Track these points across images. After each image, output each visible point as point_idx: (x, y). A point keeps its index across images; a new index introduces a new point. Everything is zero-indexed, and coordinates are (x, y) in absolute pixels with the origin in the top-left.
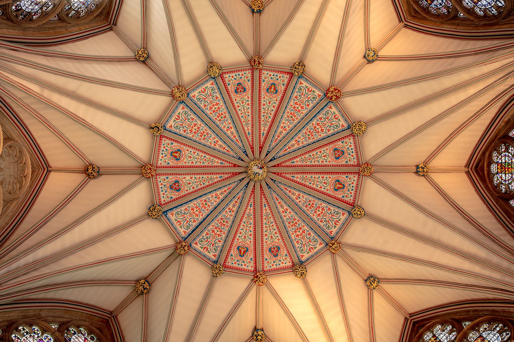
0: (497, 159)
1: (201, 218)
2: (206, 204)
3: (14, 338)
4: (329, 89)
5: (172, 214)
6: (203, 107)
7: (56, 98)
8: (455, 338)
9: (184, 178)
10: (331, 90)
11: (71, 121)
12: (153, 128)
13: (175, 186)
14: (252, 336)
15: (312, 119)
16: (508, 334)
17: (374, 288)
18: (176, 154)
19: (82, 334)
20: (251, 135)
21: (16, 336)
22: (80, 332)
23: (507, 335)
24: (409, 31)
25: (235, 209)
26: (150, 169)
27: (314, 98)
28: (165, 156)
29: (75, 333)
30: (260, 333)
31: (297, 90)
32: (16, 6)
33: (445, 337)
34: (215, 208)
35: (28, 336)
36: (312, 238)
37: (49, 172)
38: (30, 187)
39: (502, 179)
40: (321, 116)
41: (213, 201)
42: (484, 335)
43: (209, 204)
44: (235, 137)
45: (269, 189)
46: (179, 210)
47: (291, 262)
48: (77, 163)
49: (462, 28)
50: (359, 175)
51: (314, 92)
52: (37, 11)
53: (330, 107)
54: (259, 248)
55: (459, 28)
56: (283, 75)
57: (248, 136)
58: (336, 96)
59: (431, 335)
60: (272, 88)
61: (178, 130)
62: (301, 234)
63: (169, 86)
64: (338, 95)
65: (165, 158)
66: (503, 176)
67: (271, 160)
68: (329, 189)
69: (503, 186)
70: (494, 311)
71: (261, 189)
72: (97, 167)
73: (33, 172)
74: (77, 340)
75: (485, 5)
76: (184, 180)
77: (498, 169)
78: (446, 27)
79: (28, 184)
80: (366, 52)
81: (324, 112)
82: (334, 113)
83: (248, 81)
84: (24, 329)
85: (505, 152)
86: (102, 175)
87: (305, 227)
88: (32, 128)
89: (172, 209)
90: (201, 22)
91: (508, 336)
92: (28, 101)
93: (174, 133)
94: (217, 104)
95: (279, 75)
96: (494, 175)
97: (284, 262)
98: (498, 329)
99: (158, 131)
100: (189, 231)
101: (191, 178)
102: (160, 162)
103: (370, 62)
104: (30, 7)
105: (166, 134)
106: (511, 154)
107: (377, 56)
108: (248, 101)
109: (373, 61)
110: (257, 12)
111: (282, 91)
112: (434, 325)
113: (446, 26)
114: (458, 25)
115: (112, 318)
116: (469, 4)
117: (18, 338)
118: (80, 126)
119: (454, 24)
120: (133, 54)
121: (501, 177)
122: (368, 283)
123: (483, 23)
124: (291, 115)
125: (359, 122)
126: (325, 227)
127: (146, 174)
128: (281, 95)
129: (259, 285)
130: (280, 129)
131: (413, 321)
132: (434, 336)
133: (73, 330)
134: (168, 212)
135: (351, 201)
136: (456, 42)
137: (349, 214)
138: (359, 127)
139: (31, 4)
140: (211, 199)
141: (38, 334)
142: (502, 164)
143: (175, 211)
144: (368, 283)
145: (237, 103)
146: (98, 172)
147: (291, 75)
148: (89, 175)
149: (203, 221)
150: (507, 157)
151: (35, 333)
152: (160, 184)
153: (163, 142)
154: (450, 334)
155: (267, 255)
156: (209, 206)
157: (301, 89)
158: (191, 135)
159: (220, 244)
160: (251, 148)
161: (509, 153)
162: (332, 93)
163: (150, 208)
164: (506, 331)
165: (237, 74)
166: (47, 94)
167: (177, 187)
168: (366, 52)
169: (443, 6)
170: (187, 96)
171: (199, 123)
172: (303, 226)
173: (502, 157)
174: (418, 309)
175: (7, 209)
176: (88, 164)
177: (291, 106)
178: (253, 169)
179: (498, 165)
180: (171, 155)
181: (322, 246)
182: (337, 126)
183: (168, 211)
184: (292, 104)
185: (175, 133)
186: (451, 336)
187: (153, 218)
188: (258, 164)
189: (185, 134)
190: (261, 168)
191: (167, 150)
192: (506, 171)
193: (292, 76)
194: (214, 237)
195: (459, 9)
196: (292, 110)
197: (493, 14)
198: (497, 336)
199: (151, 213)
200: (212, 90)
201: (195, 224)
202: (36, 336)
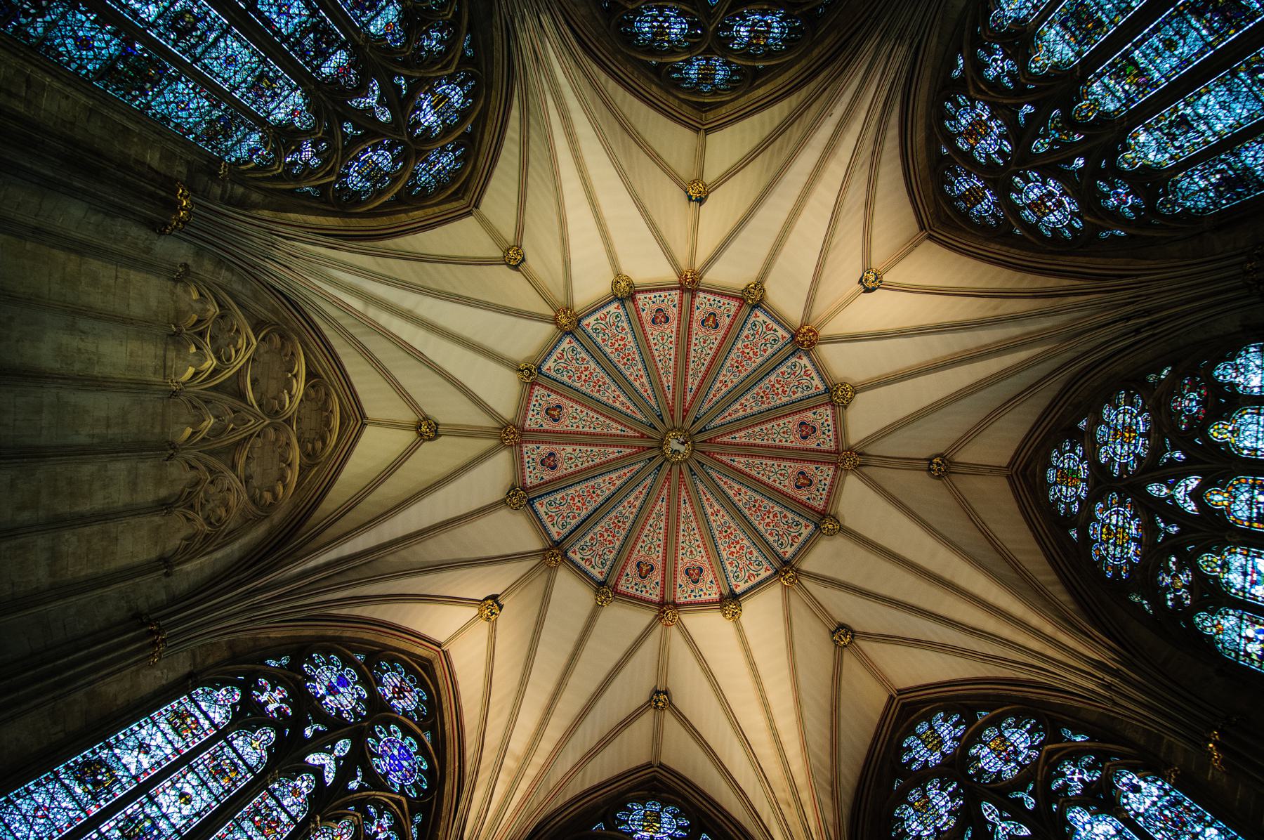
0: (1057, 461)
1: (584, 513)
2: (594, 492)
3: (306, 669)
4: (800, 329)
5: (542, 504)
6: (601, 341)
7: (384, 319)
8: (962, 735)
9: (564, 449)
10: (803, 330)
11: (402, 354)
12: (523, 371)
13: (549, 462)
14: (650, 701)
15: (769, 372)
16: (1042, 735)
17: (845, 646)
18: (554, 413)
19: (397, 672)
20: (671, 390)
21: (308, 667)
22: (394, 669)
23: (1040, 736)
24: (935, 246)
25: (638, 504)
26: (514, 433)
27: (775, 340)
28: (538, 414)
29: (388, 670)
30: (662, 697)
31: (750, 326)
32: (340, 184)
33: (947, 731)
34: (608, 500)
35: (324, 668)
36: (754, 559)
37: (364, 425)
38: (336, 446)
39: (1061, 494)
40: (784, 369)
42: (1007, 734)
43: (599, 492)
44: (646, 391)
46: (552, 499)
47: (718, 594)
48: (409, 416)
49: (1018, 251)
50: (836, 467)
51: (775, 330)
52: (368, 190)
53: (800, 358)
54: (670, 568)
55: (1012, 250)
56: (729, 301)
58: (810, 341)
59: (926, 726)
60: (711, 320)
62: (738, 552)
63: (552, 306)
64: (813, 339)
65: (536, 417)
66: (1064, 489)
67: (700, 432)
68: (787, 486)
69: (1063, 506)
70: (1026, 699)
72: (435, 423)
73: (342, 424)
74: (390, 680)
75: (1054, 223)
77: (1057, 477)
78: (994, 247)
79: (334, 442)
80: (863, 275)
81: (790, 364)
82: (805, 367)
83: (674, 306)
84: (319, 658)
85: (1069, 451)
86: (441, 435)
87: (745, 542)
88: (346, 362)
89: (543, 495)
90: (607, 212)
91: (1042, 738)
92: (345, 321)
93: (553, 379)
94: (623, 339)
95: (722, 301)
96: (1051, 485)
97: (708, 592)
98: (1028, 726)
99: (530, 375)
100: (565, 532)
101: (574, 450)
102: (528, 422)
103: (868, 290)
104: (360, 184)
105: (542, 380)
106: (1079, 457)
107: (880, 282)
108: (671, 337)
109: (873, 290)
110: (696, 200)
111: (726, 326)
112: (934, 712)
113: (992, 245)
114: (1012, 246)
115: (442, 653)
116: (1030, 217)
117: (312, 670)
118: (414, 362)
119: (1005, 244)
120: (501, 254)
121: (1060, 491)
122: (836, 638)
123: (1050, 248)
124: (736, 364)
125: (842, 385)
126: (776, 544)
128: (723, 331)
129: (666, 625)
130: (718, 385)
131: (901, 702)
132: (931, 727)
133: (385, 665)
135: (821, 508)
136: (1007, 273)
137: (816, 527)
138: (842, 392)
139: (361, 180)
140: (602, 485)
141: (338, 667)
142: (1063, 471)
143: (546, 500)
144: (836, 638)
145: (654, 339)
146: (436, 431)
147: (742, 302)
148: (421, 435)
149: (588, 518)
150: (1072, 461)
151: (334, 665)
152: (526, 456)
154: (955, 728)
155: (682, 579)
156: (598, 495)
157: (755, 325)
158: (579, 385)
159: (611, 556)
160: (670, 411)
161: (1076, 454)
162: (804, 336)
163: (509, 492)
164: (1039, 730)
165: (657, 294)
166: (372, 312)
167: (552, 463)
168: (863, 275)
169: (989, 215)
170: (578, 325)
171: (593, 366)
172: (742, 540)
173: (1064, 459)
174: (911, 684)
175: (304, 479)
176: (421, 418)
177: (738, 349)
178: (671, 445)
179: (1057, 471)
180: (547, 412)
181: (768, 573)
182: (808, 387)
183: (535, 498)
184: (739, 346)
185: (555, 380)
186: (957, 730)
187: (512, 508)
189: (569, 382)
190: (683, 444)
191: (540, 404)
192: (1068, 483)
193: (743, 305)
194: (602, 544)
195: (1013, 223)
196: (738, 356)
197: (1065, 237)
198: (1024, 736)
200: (617, 317)
201: (574, 522)
202: (335, 669)
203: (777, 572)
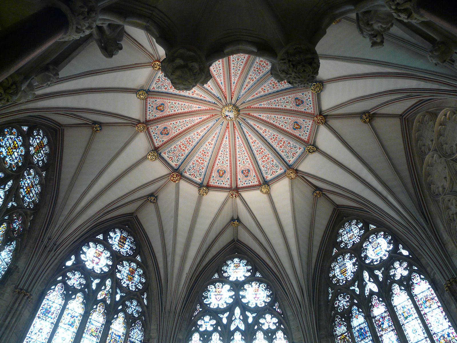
9: (291, 107)
12: (313, 151)
20: (237, 137)
41: (267, 87)
43: (270, 85)
57: (238, 136)
61: (295, 145)
71: (225, 96)
76: (292, 106)
101: (285, 106)
127: (322, 119)
140: (269, 88)
153: (307, 137)
156: (271, 84)
188: (230, 119)
190: (227, 116)
199: (320, 88)
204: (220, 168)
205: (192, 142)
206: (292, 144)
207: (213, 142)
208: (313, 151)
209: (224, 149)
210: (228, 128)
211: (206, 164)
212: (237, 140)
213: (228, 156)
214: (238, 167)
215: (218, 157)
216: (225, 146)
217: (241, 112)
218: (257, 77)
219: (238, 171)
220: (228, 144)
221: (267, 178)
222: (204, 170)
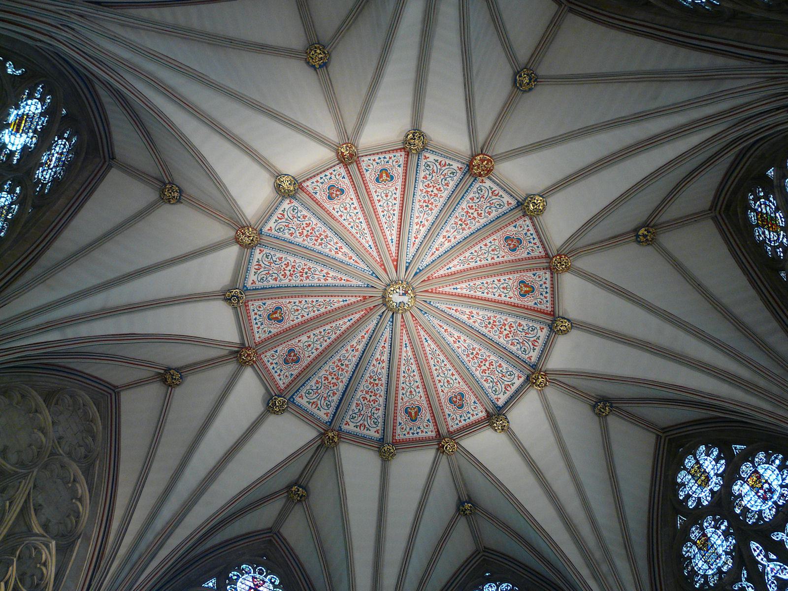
2: (342, 365)
5: (301, 397)
9: (299, 341)
20: (374, 249)
41: (350, 357)
43: (346, 362)
45: (425, 315)
76: (299, 344)
101: (309, 337)
134: (294, 397)
140: (347, 355)
156: (347, 366)
188: (398, 290)
190: (404, 294)
203: (528, 378)
204: (390, 185)
205: (456, 223)
206: (271, 280)
207: (415, 227)
208: (230, 299)
209: (391, 219)
210: (393, 261)
211: (421, 186)
212: (371, 243)
213: (380, 209)
214: (353, 196)
215: (398, 202)
216: (390, 227)
217: (380, 301)
218: (372, 368)
219: (352, 190)
220: (386, 230)
221: (290, 201)
222: (422, 174)
